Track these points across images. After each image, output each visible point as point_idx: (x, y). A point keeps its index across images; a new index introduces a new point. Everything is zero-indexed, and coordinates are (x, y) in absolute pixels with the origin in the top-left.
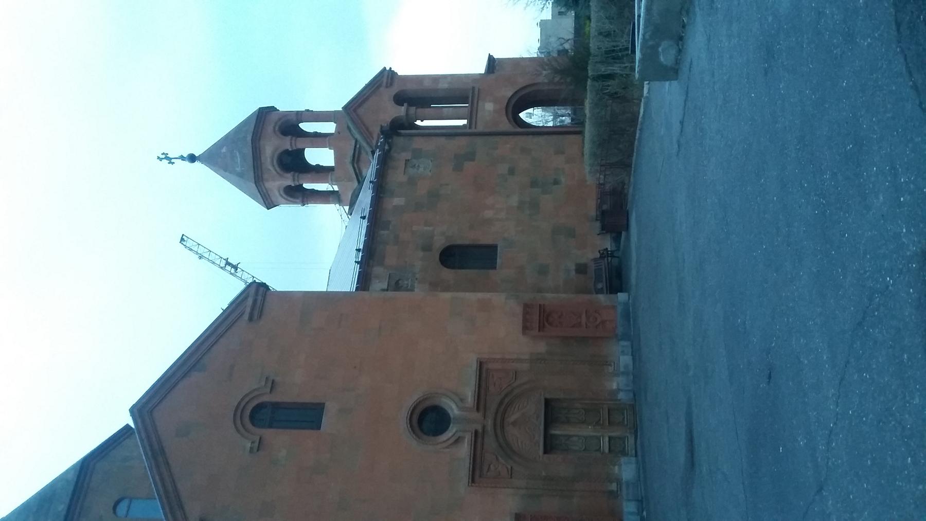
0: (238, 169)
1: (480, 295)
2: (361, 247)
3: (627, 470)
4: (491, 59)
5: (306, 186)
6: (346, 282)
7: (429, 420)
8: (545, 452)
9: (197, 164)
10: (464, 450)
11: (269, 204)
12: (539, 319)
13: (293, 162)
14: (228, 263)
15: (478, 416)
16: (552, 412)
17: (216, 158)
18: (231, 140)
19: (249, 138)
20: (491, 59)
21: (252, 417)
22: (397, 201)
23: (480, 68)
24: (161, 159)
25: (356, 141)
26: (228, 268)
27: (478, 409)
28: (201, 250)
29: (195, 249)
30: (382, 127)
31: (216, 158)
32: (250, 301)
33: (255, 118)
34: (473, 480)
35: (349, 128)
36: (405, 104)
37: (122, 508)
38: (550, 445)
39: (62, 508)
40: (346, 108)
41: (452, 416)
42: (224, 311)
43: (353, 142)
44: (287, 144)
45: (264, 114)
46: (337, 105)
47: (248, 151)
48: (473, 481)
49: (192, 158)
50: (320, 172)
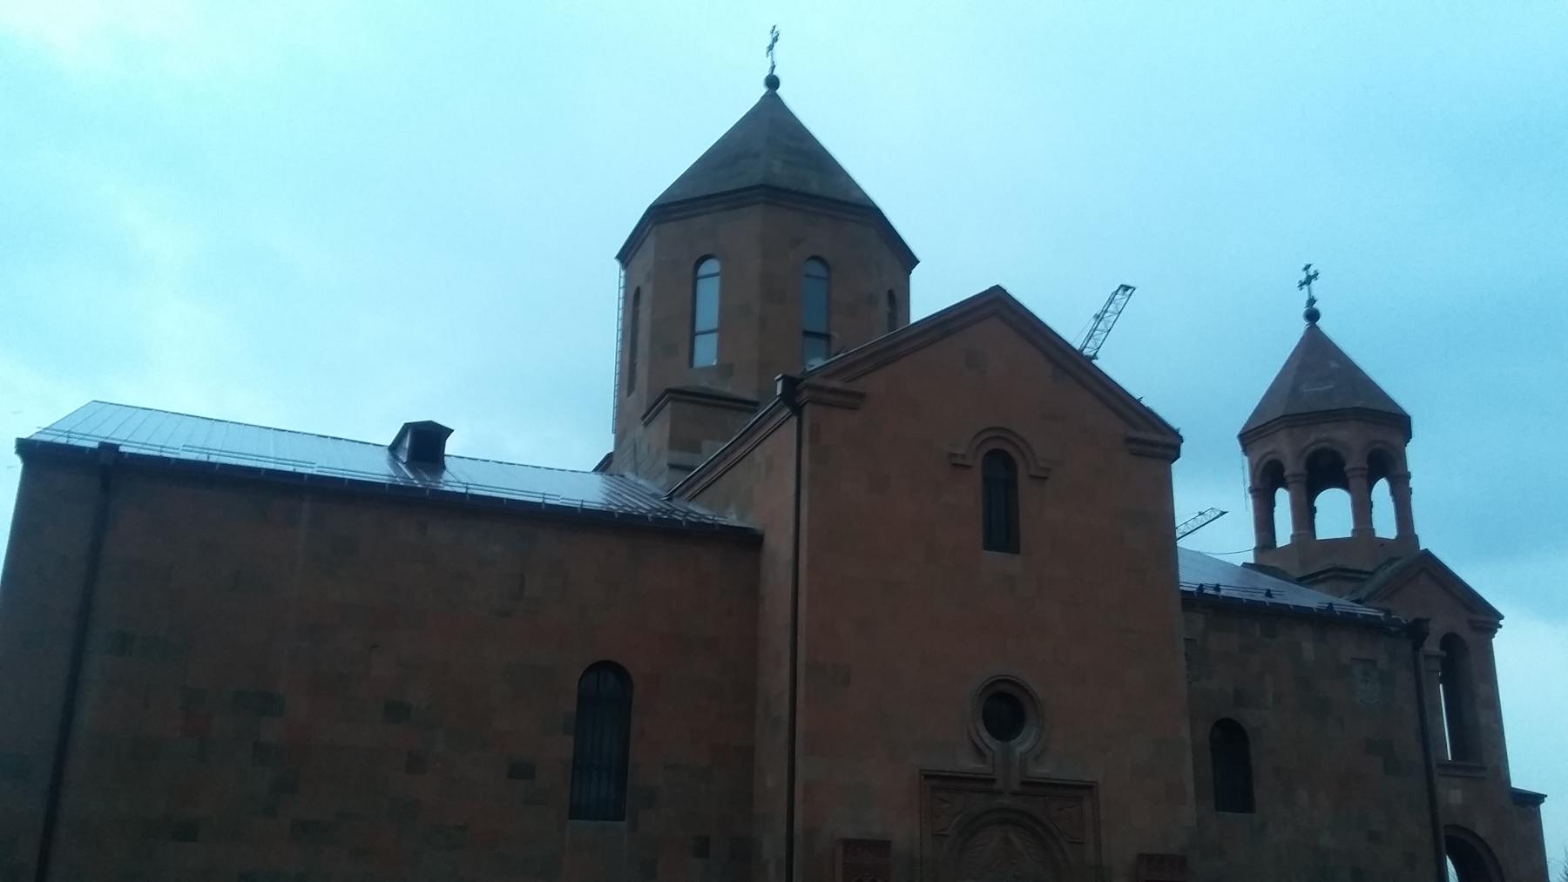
1: (1190, 788)
2: (1223, 593)
5: (1283, 498)
6: (1189, 577)
10: (968, 763)
11: (1248, 438)
13: (1323, 471)
17: (1317, 355)
19: (1358, 404)
21: (994, 454)
24: (1307, 267)
27: (1023, 783)
29: (1111, 308)
30: (1428, 620)
31: (1317, 355)
32: (1156, 437)
34: (929, 776)
35: (1391, 561)
36: (1444, 653)
37: (816, 269)
40: (1427, 554)
42: (1138, 401)
44: (1355, 462)
45: (1400, 424)
46: (1429, 539)
47: (1336, 404)
48: (926, 777)
49: (1312, 316)
50: (1305, 516)
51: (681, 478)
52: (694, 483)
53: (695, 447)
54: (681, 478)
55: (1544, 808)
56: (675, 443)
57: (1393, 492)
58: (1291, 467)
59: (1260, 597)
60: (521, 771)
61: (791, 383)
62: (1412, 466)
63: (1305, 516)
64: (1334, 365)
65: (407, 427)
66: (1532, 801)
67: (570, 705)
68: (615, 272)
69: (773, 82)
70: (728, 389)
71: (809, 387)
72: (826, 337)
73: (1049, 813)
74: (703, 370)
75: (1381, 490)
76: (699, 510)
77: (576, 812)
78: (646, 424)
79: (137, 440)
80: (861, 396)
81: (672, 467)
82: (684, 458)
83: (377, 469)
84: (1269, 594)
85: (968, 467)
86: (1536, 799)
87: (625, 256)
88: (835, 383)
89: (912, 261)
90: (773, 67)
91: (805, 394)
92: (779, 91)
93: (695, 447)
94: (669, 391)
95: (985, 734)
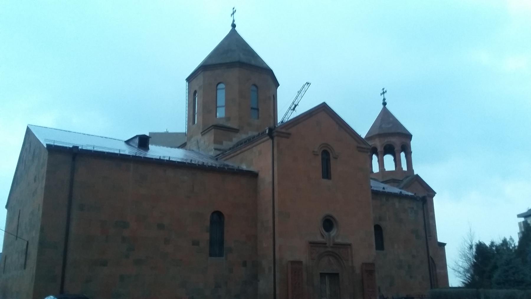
0: (383, 126)
7: (329, 223)
8: (321, 274)
9: (382, 106)
10: (320, 239)
12: (369, 270)
14: (296, 106)
15: (331, 245)
16: (334, 276)
17: (386, 116)
18: (396, 123)
19: (399, 131)
22: (397, 205)
23: (440, 239)
24: (383, 89)
25: (402, 181)
26: (293, 106)
27: (334, 244)
28: (302, 93)
31: (386, 116)
33: (404, 132)
34: (310, 243)
35: (407, 177)
37: (254, 88)
38: (322, 275)
39: (253, 62)
40: (417, 175)
41: (331, 233)
42: (360, 136)
43: (401, 179)
45: (409, 136)
46: (417, 171)
47: (393, 130)
49: (385, 104)
51: (218, 152)
52: (222, 153)
53: (221, 143)
54: (218, 152)
55: (446, 247)
56: (216, 142)
57: (406, 156)
59: (381, 190)
60: (196, 243)
61: (271, 130)
62: (413, 149)
63: (381, 163)
64: (391, 119)
65: (137, 136)
66: (443, 245)
67: (208, 223)
68: (184, 85)
69: (234, 26)
70: (229, 125)
71: (277, 132)
72: (258, 109)
73: (339, 252)
74: (221, 119)
77: (211, 255)
78: (202, 135)
79: (84, 144)
80: (289, 134)
81: (215, 149)
82: (219, 146)
83: (126, 150)
84: (384, 188)
85: (318, 155)
86: (443, 245)
87: (189, 79)
88: (284, 130)
89: (277, 85)
90: (234, 21)
91: (275, 134)
92: (236, 28)
93: (221, 143)
94: (213, 126)
95: (324, 231)
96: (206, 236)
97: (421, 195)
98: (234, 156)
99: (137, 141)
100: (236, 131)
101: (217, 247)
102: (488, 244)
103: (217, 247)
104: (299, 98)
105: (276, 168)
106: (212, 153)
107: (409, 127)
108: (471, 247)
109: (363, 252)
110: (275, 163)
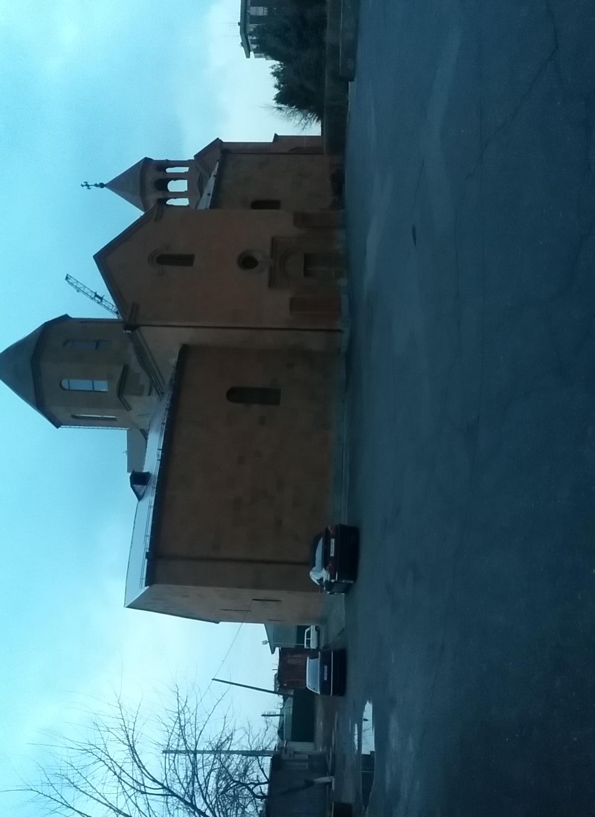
3: (343, 282)
4: (276, 135)
7: (247, 262)
10: (265, 275)
14: (96, 296)
16: (308, 260)
17: (118, 185)
20: (276, 135)
28: (79, 286)
31: (118, 185)
38: (307, 274)
40: (195, 156)
44: (160, 175)
45: (147, 161)
46: (189, 155)
51: (154, 391)
52: (155, 386)
54: (154, 391)
55: (279, 134)
56: (140, 394)
58: (160, 195)
59: (210, 197)
75: (169, 170)
76: (168, 375)
79: (143, 545)
81: (149, 394)
83: (150, 499)
96: (256, 408)
97: (218, 154)
98: (160, 373)
99: (138, 487)
100: (126, 369)
101: (268, 396)
102: (277, 91)
103: (268, 396)
104: (86, 290)
105: (176, 324)
106: (154, 398)
107: (134, 159)
108: (280, 109)
109: (281, 224)
110: (170, 324)
